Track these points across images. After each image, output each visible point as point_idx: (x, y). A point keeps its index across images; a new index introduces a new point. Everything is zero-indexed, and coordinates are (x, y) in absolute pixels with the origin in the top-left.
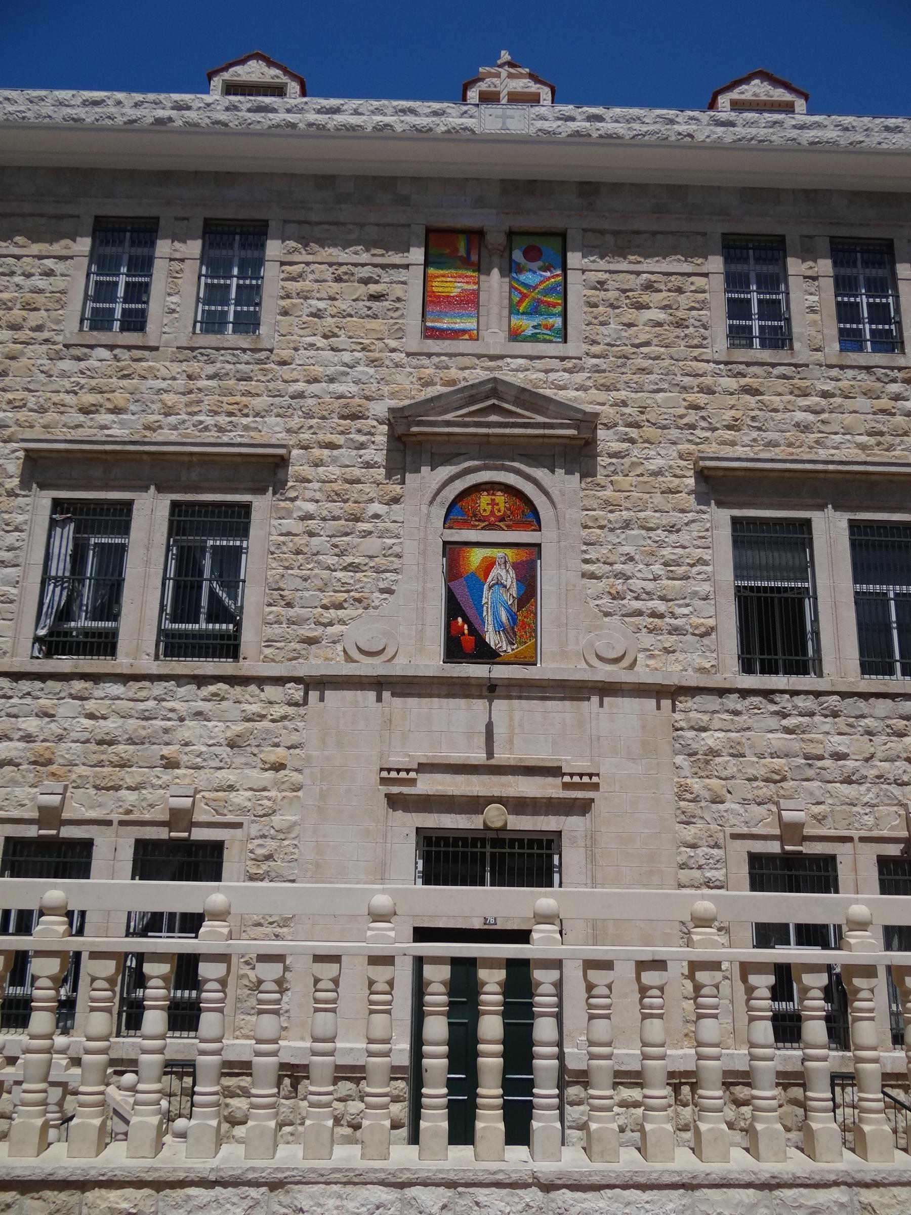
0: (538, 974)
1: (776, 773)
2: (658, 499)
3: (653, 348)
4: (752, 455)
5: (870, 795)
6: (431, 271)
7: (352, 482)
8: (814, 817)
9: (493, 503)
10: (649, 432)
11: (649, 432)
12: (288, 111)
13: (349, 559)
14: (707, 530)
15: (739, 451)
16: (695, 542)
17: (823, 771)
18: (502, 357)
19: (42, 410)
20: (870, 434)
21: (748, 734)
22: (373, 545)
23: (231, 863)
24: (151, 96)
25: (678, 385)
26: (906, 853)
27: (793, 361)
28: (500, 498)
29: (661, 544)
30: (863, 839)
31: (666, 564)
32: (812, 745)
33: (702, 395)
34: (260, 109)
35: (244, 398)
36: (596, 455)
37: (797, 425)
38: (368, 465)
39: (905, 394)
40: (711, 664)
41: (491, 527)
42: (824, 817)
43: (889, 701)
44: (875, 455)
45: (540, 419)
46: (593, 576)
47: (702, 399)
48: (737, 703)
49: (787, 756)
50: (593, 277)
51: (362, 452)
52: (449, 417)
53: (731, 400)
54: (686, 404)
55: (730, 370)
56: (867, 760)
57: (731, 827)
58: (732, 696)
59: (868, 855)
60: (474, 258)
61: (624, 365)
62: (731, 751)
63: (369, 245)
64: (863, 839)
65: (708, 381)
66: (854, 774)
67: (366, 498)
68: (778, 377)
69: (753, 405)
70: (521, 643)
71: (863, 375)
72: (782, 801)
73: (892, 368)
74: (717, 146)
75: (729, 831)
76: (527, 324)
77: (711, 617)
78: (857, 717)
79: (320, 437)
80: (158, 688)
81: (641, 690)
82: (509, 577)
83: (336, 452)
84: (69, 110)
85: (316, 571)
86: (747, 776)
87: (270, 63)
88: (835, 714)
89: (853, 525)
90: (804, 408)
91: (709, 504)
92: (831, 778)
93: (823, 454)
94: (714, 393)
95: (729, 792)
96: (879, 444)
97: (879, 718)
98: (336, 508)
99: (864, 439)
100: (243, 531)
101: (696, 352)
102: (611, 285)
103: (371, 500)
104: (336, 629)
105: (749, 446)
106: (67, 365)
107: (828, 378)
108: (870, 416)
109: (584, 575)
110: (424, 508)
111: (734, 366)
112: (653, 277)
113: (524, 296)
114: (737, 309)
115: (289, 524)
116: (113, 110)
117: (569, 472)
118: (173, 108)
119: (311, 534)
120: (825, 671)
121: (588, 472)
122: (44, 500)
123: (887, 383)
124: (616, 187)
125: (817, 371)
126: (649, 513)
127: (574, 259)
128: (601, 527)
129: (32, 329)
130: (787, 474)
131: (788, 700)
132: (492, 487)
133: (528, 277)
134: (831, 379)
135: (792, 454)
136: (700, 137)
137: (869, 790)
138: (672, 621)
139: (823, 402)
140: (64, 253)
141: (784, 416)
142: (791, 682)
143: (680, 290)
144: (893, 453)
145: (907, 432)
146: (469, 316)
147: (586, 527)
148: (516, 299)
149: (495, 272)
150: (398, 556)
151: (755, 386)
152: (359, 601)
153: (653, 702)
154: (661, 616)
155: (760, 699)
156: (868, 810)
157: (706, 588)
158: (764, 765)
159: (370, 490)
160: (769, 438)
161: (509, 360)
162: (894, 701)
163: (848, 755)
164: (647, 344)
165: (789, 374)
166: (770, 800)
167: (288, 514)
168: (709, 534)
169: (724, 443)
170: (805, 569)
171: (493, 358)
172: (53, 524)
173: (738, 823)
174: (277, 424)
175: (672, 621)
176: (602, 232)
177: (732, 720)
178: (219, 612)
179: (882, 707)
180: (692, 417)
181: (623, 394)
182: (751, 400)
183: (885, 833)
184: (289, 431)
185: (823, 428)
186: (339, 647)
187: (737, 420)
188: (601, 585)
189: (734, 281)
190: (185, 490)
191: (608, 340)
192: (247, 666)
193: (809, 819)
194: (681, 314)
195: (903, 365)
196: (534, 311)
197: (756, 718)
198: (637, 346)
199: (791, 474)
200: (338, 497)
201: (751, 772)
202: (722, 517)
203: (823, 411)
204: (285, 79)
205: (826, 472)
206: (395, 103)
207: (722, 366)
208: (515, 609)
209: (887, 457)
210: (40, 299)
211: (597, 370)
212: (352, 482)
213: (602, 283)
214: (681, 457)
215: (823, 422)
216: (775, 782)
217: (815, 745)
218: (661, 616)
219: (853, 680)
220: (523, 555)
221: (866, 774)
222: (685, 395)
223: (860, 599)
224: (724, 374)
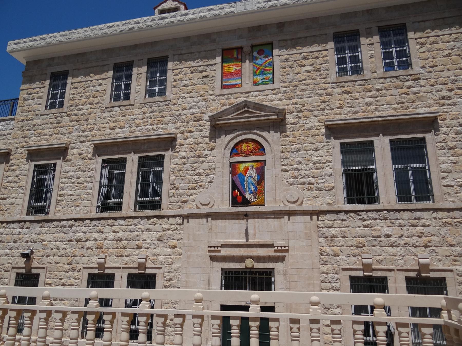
0: (271, 324)
1: (361, 244)
2: (310, 139)
3: (307, 81)
4: (348, 118)
5: (402, 252)
6: (225, 64)
7: (198, 144)
8: (377, 261)
9: (248, 146)
10: (306, 113)
11: (306, 113)
12: (171, 17)
13: (197, 172)
14: (330, 149)
15: (343, 117)
16: (326, 154)
17: (381, 242)
18: (250, 92)
19: (99, 130)
20: (398, 104)
21: (349, 228)
22: (205, 165)
23: (159, 282)
24: (128, 21)
25: (317, 94)
26: (419, 275)
27: (364, 78)
28: (250, 144)
29: (312, 156)
30: (398, 270)
31: (314, 164)
32: (376, 232)
33: (327, 96)
35: (161, 118)
36: (286, 125)
37: (366, 103)
38: (203, 137)
39: (413, 85)
40: (333, 201)
41: (247, 155)
42: (382, 261)
43: (409, 213)
44: (401, 112)
45: (263, 113)
46: (286, 170)
47: (327, 98)
48: (344, 216)
49: (365, 236)
50: (283, 58)
51: (201, 133)
52: (230, 117)
53: (339, 97)
54: (320, 101)
55: (338, 85)
56: (400, 237)
57: (342, 265)
58: (341, 213)
59: (402, 276)
60: (240, 57)
61: (296, 89)
62: (342, 235)
63: (202, 59)
64: (398, 270)
65: (329, 91)
66: (394, 243)
67: (203, 149)
68: (358, 85)
70: (259, 198)
71: (394, 80)
72: (362, 255)
73: (407, 76)
75: (341, 267)
76: (259, 79)
77: (332, 183)
78: (395, 220)
79: (187, 129)
80: (135, 221)
82: (254, 173)
83: (192, 134)
84: (103, 31)
85: (186, 177)
86: (348, 245)
88: (386, 219)
89: (391, 141)
90: (369, 96)
91: (330, 139)
92: (384, 245)
93: (378, 114)
94: (332, 95)
95: (341, 252)
96: (402, 107)
97: (405, 220)
98: (193, 154)
99: (396, 106)
101: (324, 80)
102: (290, 59)
103: (205, 150)
104: (194, 197)
105: (346, 114)
106: (106, 114)
107: (379, 83)
108: (398, 96)
109: (282, 170)
110: (223, 151)
111: (340, 83)
112: (306, 54)
113: (259, 68)
114: (341, 61)
115: (178, 161)
116: (116, 28)
117: (275, 132)
118: (134, 24)
119: (184, 164)
120: (381, 201)
121: (283, 131)
122: (100, 160)
123: (405, 82)
124: (291, 23)
125: (374, 81)
126: (307, 144)
127: (276, 52)
128: (289, 152)
129: (96, 104)
130: (362, 124)
131: (365, 214)
132: (247, 140)
133: (259, 62)
134: (381, 84)
135: (365, 115)
137: (401, 249)
138: (317, 185)
139: (377, 93)
140: (105, 77)
141: (361, 101)
142: (366, 207)
143: (317, 57)
144: (409, 110)
145: (414, 101)
146: (238, 79)
147: (283, 152)
148: (255, 70)
149: (247, 61)
150: (214, 169)
152: (201, 186)
153: (309, 217)
154: (313, 184)
155: (353, 214)
156: (401, 258)
157: (330, 171)
158: (356, 241)
159: (204, 146)
160: (355, 110)
161: (252, 93)
162: (411, 212)
163: (392, 235)
164: (305, 80)
165: (362, 84)
166: (359, 255)
167: (176, 157)
168: (331, 150)
169: (336, 114)
170: (372, 161)
171: (246, 93)
172: (102, 167)
173: (345, 264)
174: (172, 126)
175: (317, 185)
176: (286, 40)
177: (342, 223)
179: (406, 215)
180: (323, 105)
181: (296, 100)
182: (347, 96)
183: (409, 267)
184: (176, 128)
185: (377, 103)
186: (194, 203)
187: (341, 105)
189: (339, 50)
190: (143, 152)
191: (290, 80)
192: (164, 212)
193: (375, 262)
194: (318, 66)
195: (412, 73)
196: (262, 73)
197: (352, 222)
198: (301, 81)
199: (364, 124)
200: (193, 149)
201: (350, 243)
202: (336, 144)
203: (377, 97)
205: (378, 121)
206: (207, 8)
207: (335, 84)
208: (256, 185)
209: (406, 112)
210: (98, 94)
212: (198, 144)
213: (286, 59)
214: (319, 121)
215: (377, 101)
216: (360, 247)
217: (377, 232)
218: (313, 184)
219: (392, 204)
220: (259, 165)
221: (400, 243)
222: (320, 97)
223: (397, 171)
224: (335, 87)
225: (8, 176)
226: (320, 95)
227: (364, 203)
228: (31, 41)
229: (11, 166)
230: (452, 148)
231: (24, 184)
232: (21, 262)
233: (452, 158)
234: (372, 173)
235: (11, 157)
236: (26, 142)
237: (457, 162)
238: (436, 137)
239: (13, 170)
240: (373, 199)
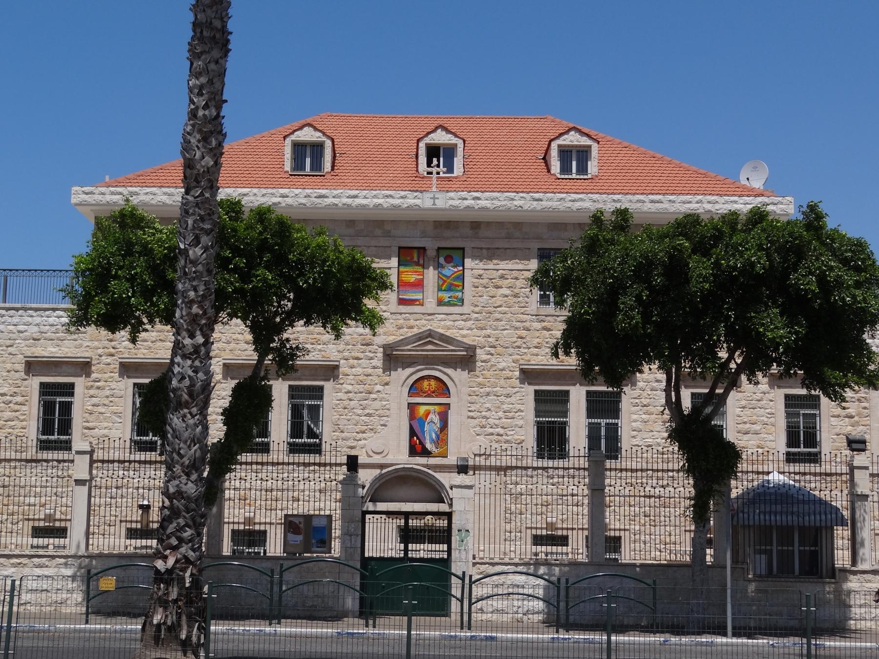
2: (502, 382)
3: (503, 308)
6: (402, 269)
7: (367, 376)
9: (430, 385)
10: (499, 349)
11: (499, 349)
12: (334, 197)
13: (367, 411)
18: (434, 314)
19: (228, 342)
22: (377, 404)
24: (270, 191)
28: (433, 382)
29: (502, 403)
34: (320, 197)
35: (318, 336)
36: (475, 362)
38: (374, 368)
41: (429, 396)
46: (472, 418)
47: (524, 333)
50: (477, 272)
51: (372, 361)
52: (409, 347)
53: (537, 334)
60: (421, 262)
61: (489, 317)
65: (527, 324)
67: (374, 383)
69: (547, 336)
70: (441, 448)
76: (446, 296)
79: (353, 354)
81: (491, 468)
82: (436, 419)
83: (360, 362)
85: (353, 417)
87: (316, 129)
94: (530, 330)
98: (361, 388)
100: (321, 398)
101: (523, 310)
102: (485, 276)
103: (376, 384)
109: (468, 417)
110: (399, 389)
112: (504, 272)
113: (445, 281)
116: (252, 198)
117: (463, 370)
118: (280, 197)
119: (351, 400)
124: (488, 224)
126: (498, 389)
127: (468, 262)
128: (477, 395)
132: (429, 377)
136: (526, 208)
138: (507, 438)
143: (517, 279)
146: (420, 292)
147: (470, 395)
148: (441, 283)
149: (431, 268)
150: (388, 409)
151: (549, 327)
152: (372, 430)
154: (502, 435)
157: (521, 423)
161: (437, 316)
164: (500, 306)
167: (340, 391)
170: (565, 413)
171: (430, 315)
174: (333, 348)
175: (507, 438)
176: (481, 249)
178: (312, 434)
181: (489, 332)
184: (339, 351)
186: (364, 450)
188: (476, 421)
190: (295, 379)
191: (482, 305)
194: (516, 291)
196: (449, 289)
198: (496, 307)
204: (324, 139)
206: (383, 192)
207: (534, 317)
208: (439, 433)
211: (477, 320)
212: (367, 376)
213: (480, 276)
214: (513, 362)
218: (502, 435)
220: (442, 409)
225: (92, 397)
226: (517, 329)
227: (563, 427)
228: (112, 193)
229: (94, 381)
230: (645, 406)
231: (120, 409)
232: (137, 515)
233: (644, 416)
234: (565, 428)
235: (93, 368)
236: (114, 348)
237: (648, 421)
238: (632, 392)
239: (98, 388)
240: (563, 454)
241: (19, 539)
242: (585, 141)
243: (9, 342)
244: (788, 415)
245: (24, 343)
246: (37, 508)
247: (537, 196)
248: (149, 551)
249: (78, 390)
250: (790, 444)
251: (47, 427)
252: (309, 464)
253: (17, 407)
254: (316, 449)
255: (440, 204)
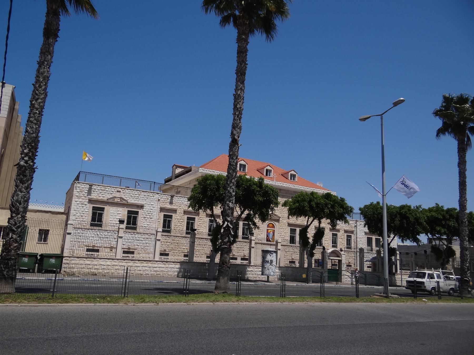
28: (271, 225)
29: (284, 231)
74: (293, 188)
82: (272, 233)
87: (244, 161)
124: (283, 190)
132: (271, 223)
181: (282, 214)
188: (279, 234)
228: (209, 171)
231: (206, 225)
239: (201, 219)
241: (181, 257)
242: (295, 173)
243: (180, 205)
244: (333, 237)
245: (184, 206)
246: (185, 249)
247: (294, 185)
248: (208, 262)
249: (196, 219)
250: (347, 245)
251: (93, 219)
252: (247, 242)
253: (181, 223)
254: (169, 232)
255: (276, 184)
